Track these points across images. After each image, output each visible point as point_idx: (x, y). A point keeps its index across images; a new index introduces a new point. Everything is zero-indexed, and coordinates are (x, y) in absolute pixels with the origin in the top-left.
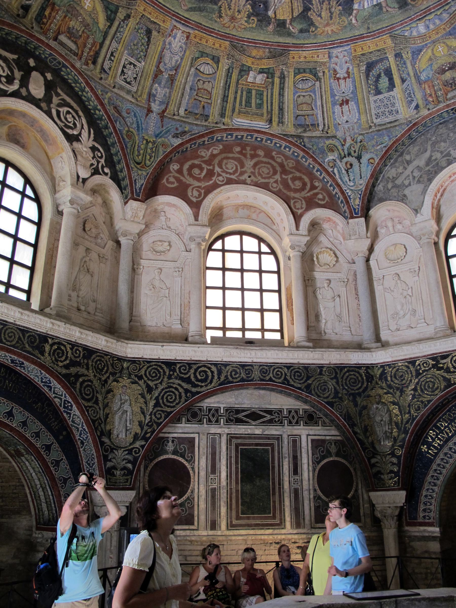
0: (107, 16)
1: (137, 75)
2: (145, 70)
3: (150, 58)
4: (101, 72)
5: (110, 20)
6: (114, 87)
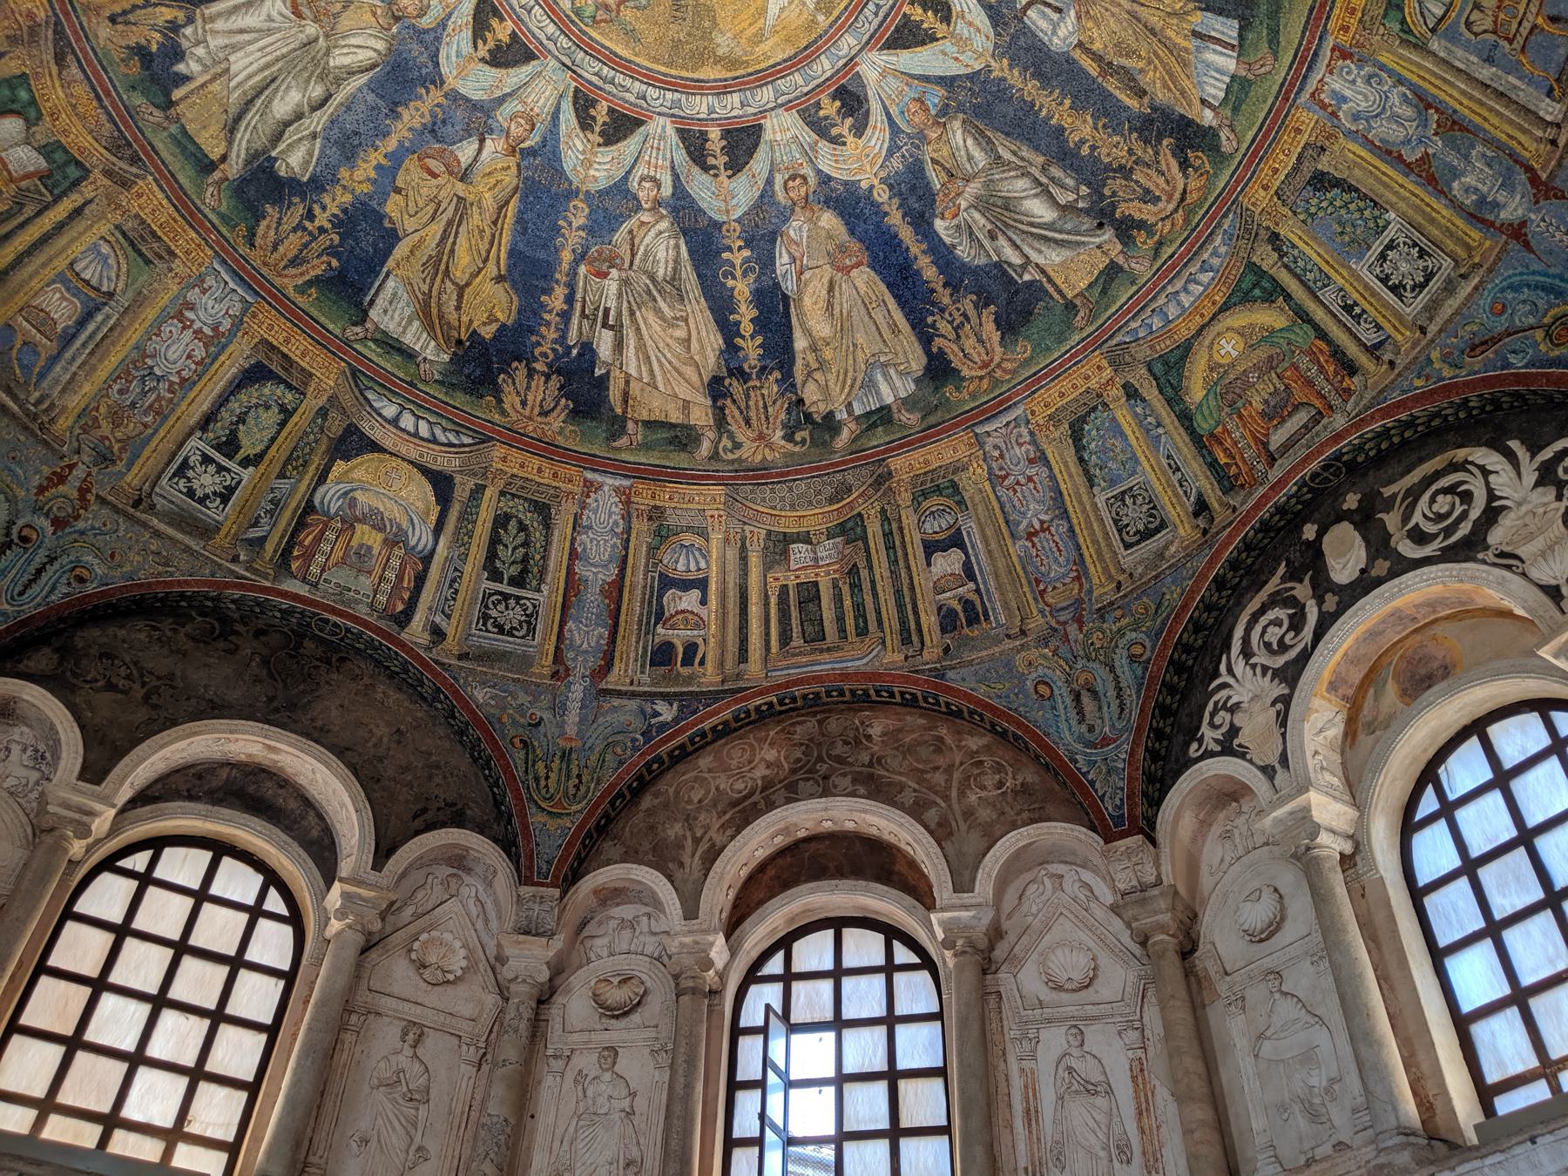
0: (1264, 301)
1: (1415, 245)
2: (1411, 212)
3: (1382, 190)
4: (1378, 358)
5: (1274, 292)
6: (1423, 330)
